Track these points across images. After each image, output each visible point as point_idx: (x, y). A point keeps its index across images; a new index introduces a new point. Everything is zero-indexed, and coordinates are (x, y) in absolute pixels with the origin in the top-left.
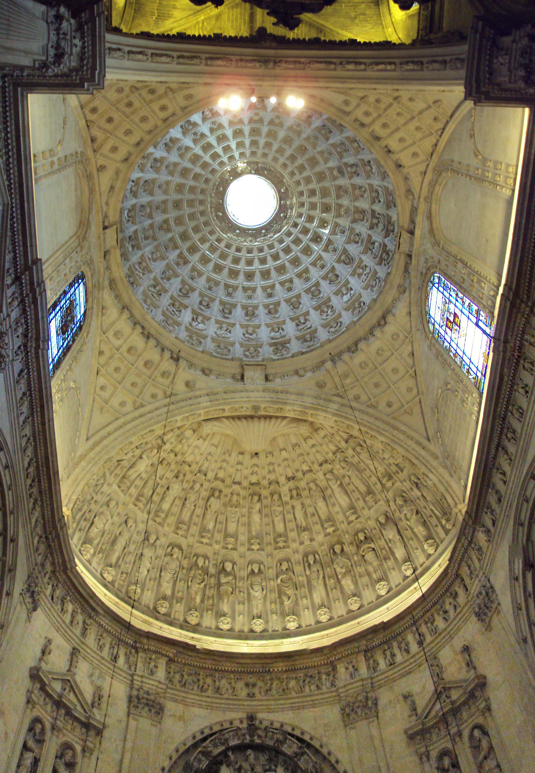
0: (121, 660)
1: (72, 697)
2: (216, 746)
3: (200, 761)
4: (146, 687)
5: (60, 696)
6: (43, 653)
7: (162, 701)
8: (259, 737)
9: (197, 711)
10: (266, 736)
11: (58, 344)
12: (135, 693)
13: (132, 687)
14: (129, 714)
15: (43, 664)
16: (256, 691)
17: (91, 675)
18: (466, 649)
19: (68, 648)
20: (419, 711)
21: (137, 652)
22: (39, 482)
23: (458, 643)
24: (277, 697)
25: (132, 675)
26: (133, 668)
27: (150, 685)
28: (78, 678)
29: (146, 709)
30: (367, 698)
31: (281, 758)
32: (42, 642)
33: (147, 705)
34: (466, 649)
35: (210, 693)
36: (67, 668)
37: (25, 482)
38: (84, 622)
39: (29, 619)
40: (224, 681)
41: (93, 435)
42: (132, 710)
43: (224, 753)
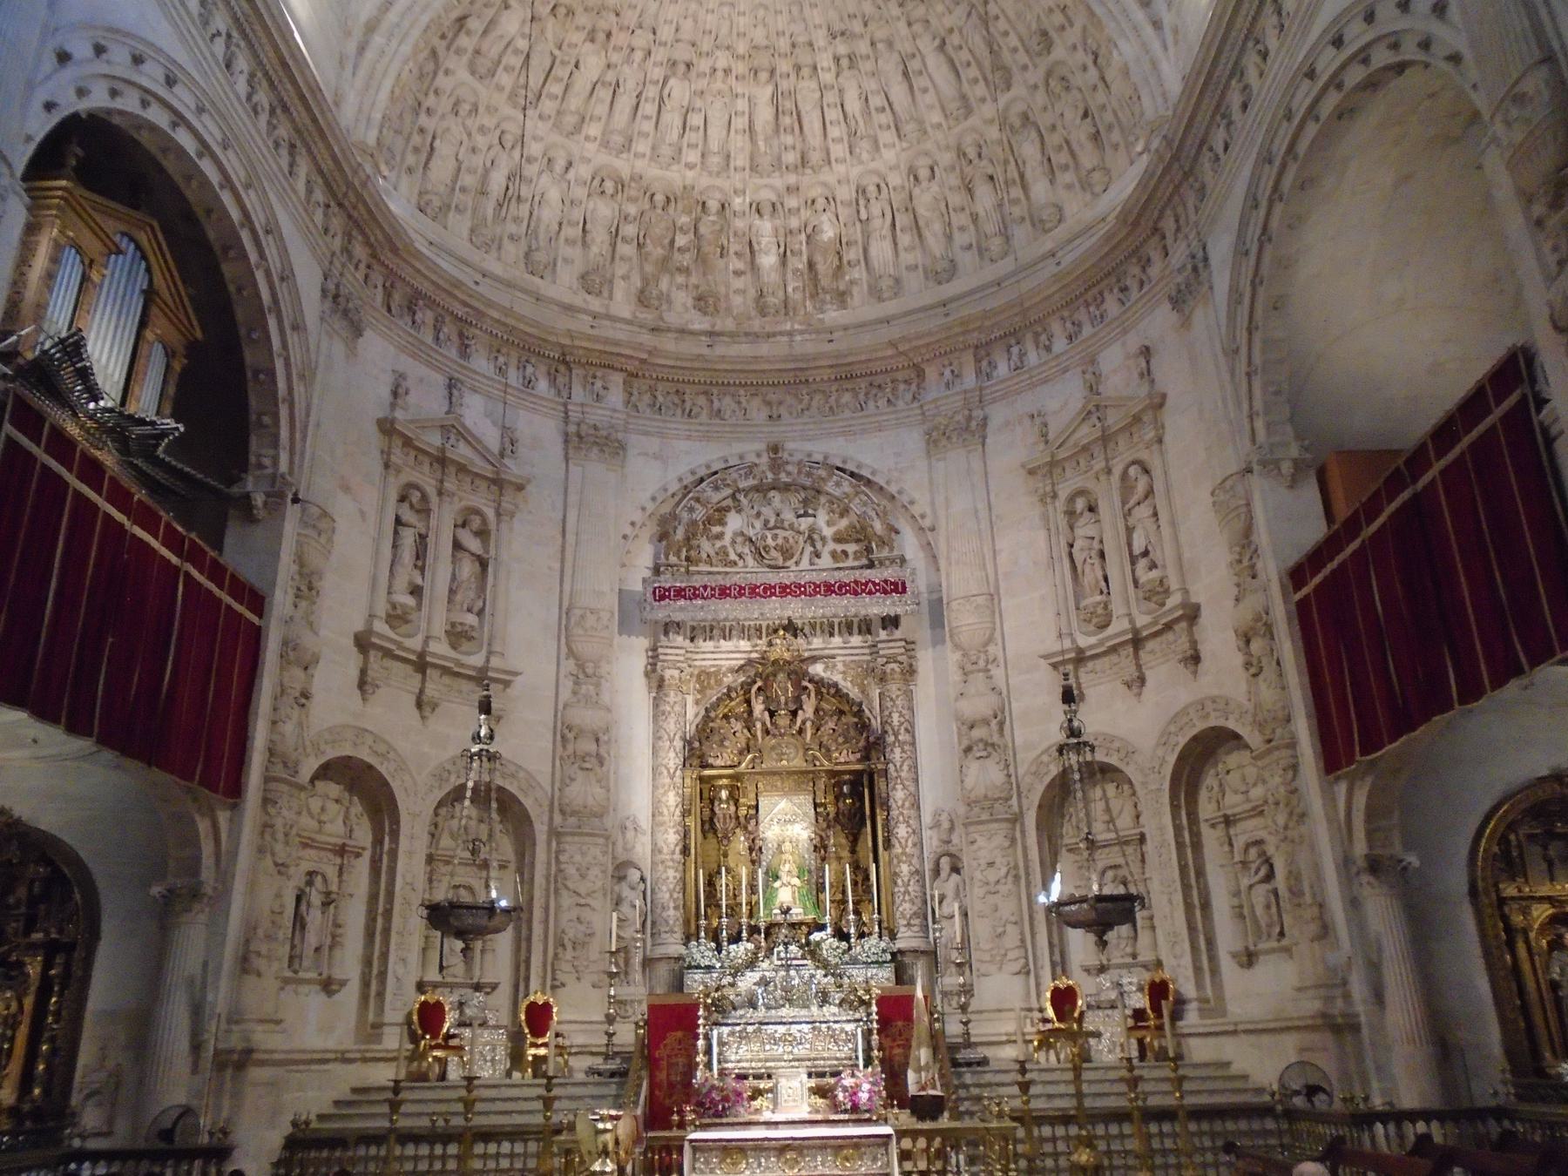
0: (543, 385)
3: (691, 510)
5: (443, 450)
6: (395, 394)
7: (620, 436)
8: (789, 474)
9: (683, 445)
10: (799, 472)
12: (572, 429)
14: (567, 460)
15: (399, 414)
16: (783, 411)
18: (1146, 352)
19: (440, 380)
20: (1051, 436)
22: (286, 109)
23: (1134, 342)
25: (565, 405)
26: (565, 394)
27: (597, 415)
28: (469, 423)
30: (969, 418)
31: (823, 499)
34: (1146, 352)
35: (704, 417)
36: (445, 408)
39: (352, 352)
40: (728, 400)
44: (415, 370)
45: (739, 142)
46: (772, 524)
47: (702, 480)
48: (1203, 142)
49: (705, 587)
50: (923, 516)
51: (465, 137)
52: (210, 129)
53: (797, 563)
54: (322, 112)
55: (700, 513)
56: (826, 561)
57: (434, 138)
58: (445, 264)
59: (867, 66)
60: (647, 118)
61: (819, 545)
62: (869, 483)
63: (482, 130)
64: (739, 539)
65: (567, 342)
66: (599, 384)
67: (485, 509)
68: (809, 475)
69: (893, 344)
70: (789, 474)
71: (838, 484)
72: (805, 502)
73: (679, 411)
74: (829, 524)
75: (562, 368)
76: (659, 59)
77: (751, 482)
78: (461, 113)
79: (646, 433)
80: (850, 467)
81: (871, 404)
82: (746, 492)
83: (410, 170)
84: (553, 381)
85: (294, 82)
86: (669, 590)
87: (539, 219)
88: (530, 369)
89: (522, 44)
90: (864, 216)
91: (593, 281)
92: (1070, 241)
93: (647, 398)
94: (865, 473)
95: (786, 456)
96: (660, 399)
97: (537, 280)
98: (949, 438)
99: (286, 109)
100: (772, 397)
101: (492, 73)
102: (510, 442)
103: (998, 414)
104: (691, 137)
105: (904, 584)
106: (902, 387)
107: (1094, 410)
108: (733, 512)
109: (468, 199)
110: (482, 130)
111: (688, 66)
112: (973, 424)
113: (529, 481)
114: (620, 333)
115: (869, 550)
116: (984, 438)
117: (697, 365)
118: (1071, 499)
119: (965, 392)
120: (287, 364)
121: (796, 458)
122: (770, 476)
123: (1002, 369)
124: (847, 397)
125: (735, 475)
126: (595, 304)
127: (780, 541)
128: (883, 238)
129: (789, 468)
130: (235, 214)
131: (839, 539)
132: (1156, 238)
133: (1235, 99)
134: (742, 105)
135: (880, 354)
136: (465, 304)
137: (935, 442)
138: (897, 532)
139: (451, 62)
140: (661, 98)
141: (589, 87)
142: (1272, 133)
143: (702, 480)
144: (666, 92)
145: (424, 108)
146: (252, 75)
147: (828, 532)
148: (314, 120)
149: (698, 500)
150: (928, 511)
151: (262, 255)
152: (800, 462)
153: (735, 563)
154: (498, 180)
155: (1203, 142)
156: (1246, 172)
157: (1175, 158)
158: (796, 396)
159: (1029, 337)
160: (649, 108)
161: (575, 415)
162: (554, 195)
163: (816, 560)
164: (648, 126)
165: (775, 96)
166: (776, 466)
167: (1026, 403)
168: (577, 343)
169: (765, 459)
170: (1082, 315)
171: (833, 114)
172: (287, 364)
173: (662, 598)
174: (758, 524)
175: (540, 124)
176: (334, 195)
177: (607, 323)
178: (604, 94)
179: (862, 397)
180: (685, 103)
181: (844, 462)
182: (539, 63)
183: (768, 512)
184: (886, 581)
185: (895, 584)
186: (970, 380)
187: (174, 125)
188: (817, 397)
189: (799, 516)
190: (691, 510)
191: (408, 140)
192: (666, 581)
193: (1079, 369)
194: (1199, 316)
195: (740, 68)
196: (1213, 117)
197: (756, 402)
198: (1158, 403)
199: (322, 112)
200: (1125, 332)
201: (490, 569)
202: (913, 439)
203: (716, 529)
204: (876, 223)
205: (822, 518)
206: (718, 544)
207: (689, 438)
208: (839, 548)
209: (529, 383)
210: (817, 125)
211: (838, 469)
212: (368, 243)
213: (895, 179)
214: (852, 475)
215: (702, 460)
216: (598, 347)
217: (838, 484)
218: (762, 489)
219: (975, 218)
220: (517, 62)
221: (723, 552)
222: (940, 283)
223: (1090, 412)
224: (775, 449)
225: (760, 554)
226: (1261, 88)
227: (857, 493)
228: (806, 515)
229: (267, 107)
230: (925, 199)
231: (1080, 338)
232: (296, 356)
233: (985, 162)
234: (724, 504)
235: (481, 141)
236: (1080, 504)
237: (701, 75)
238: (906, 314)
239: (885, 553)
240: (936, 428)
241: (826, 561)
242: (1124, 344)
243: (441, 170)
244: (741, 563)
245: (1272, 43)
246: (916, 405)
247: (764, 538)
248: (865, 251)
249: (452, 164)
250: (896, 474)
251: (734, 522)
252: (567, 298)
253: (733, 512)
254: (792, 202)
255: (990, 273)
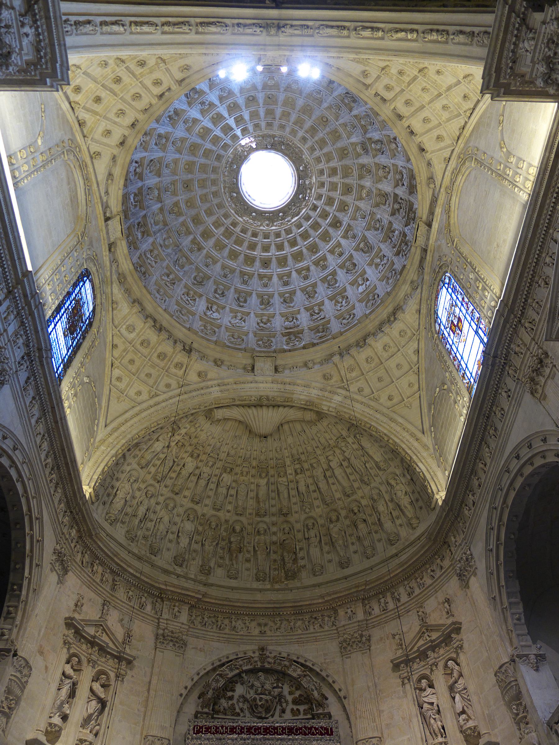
0: (149, 608)
1: (105, 638)
2: (231, 670)
3: (217, 681)
4: (171, 628)
11: (67, 345)
12: (161, 632)
13: (158, 627)
16: (266, 629)
17: (122, 620)
19: (100, 601)
21: (163, 601)
22: (58, 468)
24: (285, 633)
25: (158, 619)
26: (159, 614)
27: (174, 626)
28: (109, 624)
29: (171, 644)
32: (75, 597)
33: (172, 641)
35: (227, 631)
36: (99, 616)
37: (44, 472)
38: (114, 580)
40: (240, 622)
41: (111, 422)
42: (159, 645)
43: (239, 675)
44: (90, 594)
45: (251, 503)
46: (259, 691)
47: (223, 665)
48: (462, 502)
49: (222, 727)
50: (340, 690)
51: (131, 491)
52: (25, 471)
53: (272, 716)
54: (74, 471)
55: (222, 683)
56: (288, 715)
57: (117, 490)
58: (112, 545)
59: (308, 473)
60: (211, 490)
61: (284, 705)
62: (311, 670)
63: (139, 489)
64: (241, 700)
65: (163, 587)
66: (176, 609)
67: (110, 672)
68: (280, 664)
69: (322, 597)
70: (269, 663)
71: (295, 671)
72: (278, 680)
73: (215, 626)
74: (290, 693)
75: (159, 600)
76: (219, 466)
77: (249, 667)
78: (131, 480)
79: (197, 637)
80: (301, 660)
81: (311, 627)
82: (247, 672)
83: (104, 504)
84: (154, 608)
85: (65, 457)
86: (201, 727)
87: (158, 529)
88: (144, 599)
89: (162, 456)
90: (307, 536)
91: (179, 561)
92: (404, 549)
93: (199, 619)
94: (308, 664)
95: (268, 654)
96: (206, 619)
97: (153, 557)
98: (352, 646)
99: (58, 468)
100: (262, 621)
101: (147, 465)
102: (128, 635)
103: (376, 634)
104: (229, 499)
105: (331, 729)
106: (326, 619)
107: (426, 628)
108: (239, 684)
109: (127, 519)
110: (139, 489)
111: (231, 470)
112: (364, 639)
113: (135, 659)
114: (189, 585)
115: (312, 709)
116: (370, 646)
117: (225, 603)
118: (419, 681)
119: (359, 621)
120: (29, 583)
121: (272, 655)
122: (259, 664)
123: (377, 611)
124: (299, 623)
125: (241, 663)
126: (179, 570)
127: (263, 702)
128: (316, 546)
129: (270, 660)
130: (25, 508)
131: (295, 702)
132: (446, 546)
133: (476, 483)
134: (253, 487)
135: (315, 602)
136: (118, 565)
137: (345, 648)
138: (327, 699)
139: (130, 459)
140: (218, 481)
141: (187, 475)
142: (494, 498)
143: (223, 665)
144: (221, 479)
145: (115, 477)
146: (48, 452)
147: (290, 698)
148: (70, 474)
149: (220, 675)
150: (343, 687)
151: (31, 529)
152: (275, 657)
153: (238, 715)
154: (142, 510)
155: (462, 502)
156: (485, 514)
157: (451, 510)
158: (274, 621)
159: (388, 594)
160: (212, 486)
161: (162, 625)
162: (166, 519)
163: (283, 715)
164: (211, 493)
165: (267, 483)
166: (263, 658)
167: (392, 627)
168: (168, 588)
169: (257, 654)
170: (413, 584)
171: (293, 493)
172: (29, 583)
173: (198, 732)
174: (252, 692)
175: (164, 489)
176: (69, 507)
177: (184, 580)
178: (194, 479)
179: (307, 623)
180: (229, 484)
181: (298, 658)
182: (169, 463)
183: (257, 684)
184: (322, 727)
185: (326, 729)
186: (360, 615)
187: (11, 467)
188: (285, 622)
189: (274, 688)
190: (217, 681)
191: (106, 490)
192: (202, 722)
193: (415, 611)
194: (474, 582)
195: (253, 472)
196: (465, 492)
197: (254, 624)
198: (457, 628)
199: (74, 471)
200: (436, 592)
201: (107, 709)
202: (333, 647)
203: (229, 694)
204: (313, 540)
205: (286, 690)
206: (230, 702)
207: (219, 641)
208: (295, 707)
209: (142, 606)
210: (286, 495)
211: (295, 661)
212: (79, 531)
213: (321, 521)
214: (302, 665)
215: (225, 653)
216: (179, 591)
217: (295, 671)
218: (253, 671)
219: (359, 538)
220: (158, 463)
221: (233, 707)
222: (343, 568)
223: (423, 633)
224: (262, 649)
225: (253, 708)
226: (486, 477)
227: (305, 676)
228: (277, 687)
229: (51, 466)
230: (335, 529)
231: (414, 595)
232: (34, 580)
233: (362, 514)
234: (235, 679)
235: (138, 494)
236: (424, 683)
237: (236, 474)
238: (327, 582)
239: (320, 711)
240: (345, 641)
241: (288, 715)
242: (436, 598)
243: (118, 503)
244: (242, 714)
245: (488, 461)
246: (334, 628)
247: (255, 699)
248: (308, 552)
249: (123, 502)
250: (325, 665)
251: (240, 690)
252: (166, 567)
253: (239, 684)
254: (274, 529)
255: (367, 564)
